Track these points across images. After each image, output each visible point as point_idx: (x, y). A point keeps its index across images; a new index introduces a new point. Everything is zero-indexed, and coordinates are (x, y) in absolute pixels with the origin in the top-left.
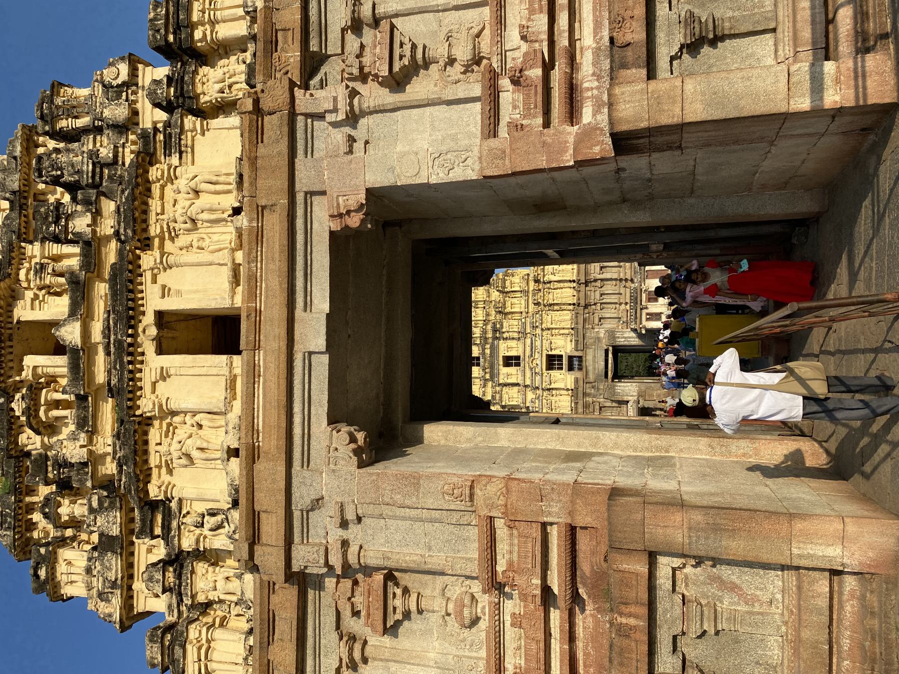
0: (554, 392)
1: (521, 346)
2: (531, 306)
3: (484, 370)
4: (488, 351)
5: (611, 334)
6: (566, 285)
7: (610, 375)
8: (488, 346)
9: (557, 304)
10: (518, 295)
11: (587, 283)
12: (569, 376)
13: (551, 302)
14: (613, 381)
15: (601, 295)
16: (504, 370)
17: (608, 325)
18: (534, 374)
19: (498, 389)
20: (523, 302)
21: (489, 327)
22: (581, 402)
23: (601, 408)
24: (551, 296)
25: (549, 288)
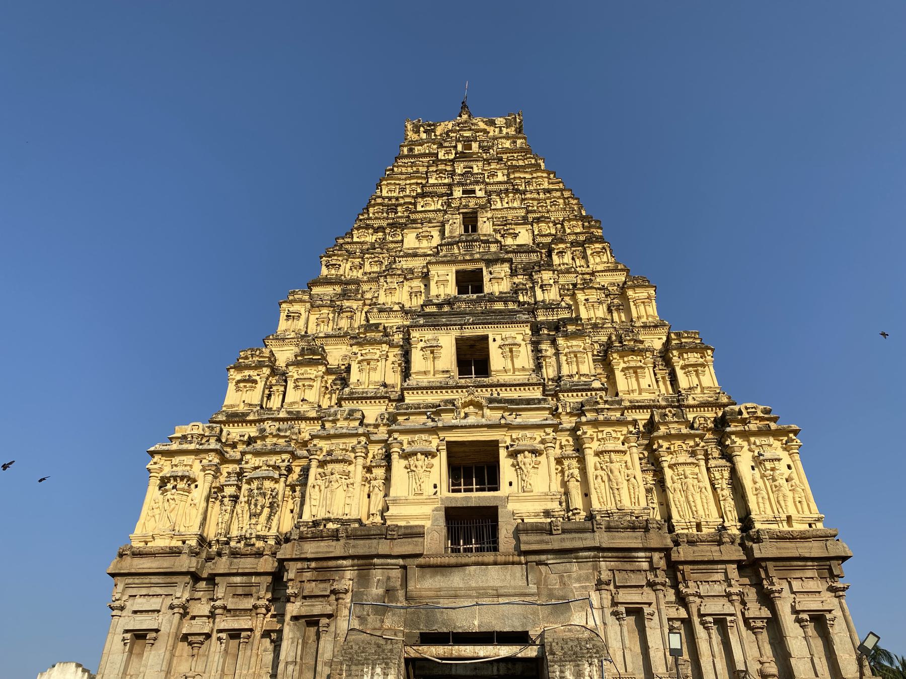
0: (380, 472)
1: (521, 377)
2: (642, 417)
3: (449, 302)
4: (499, 306)
5: (591, 649)
6: (729, 505)
7: (433, 652)
8: (511, 306)
9: (661, 483)
10: (665, 389)
11: (751, 568)
12: (428, 510)
13: (667, 460)
14: (409, 661)
15: (721, 622)
16: (447, 341)
17: (619, 637)
18: (437, 410)
19: (398, 338)
20: (646, 396)
21: (565, 315)
22: (336, 548)
23: (312, 621)
24: (683, 458)
25: (706, 454)
